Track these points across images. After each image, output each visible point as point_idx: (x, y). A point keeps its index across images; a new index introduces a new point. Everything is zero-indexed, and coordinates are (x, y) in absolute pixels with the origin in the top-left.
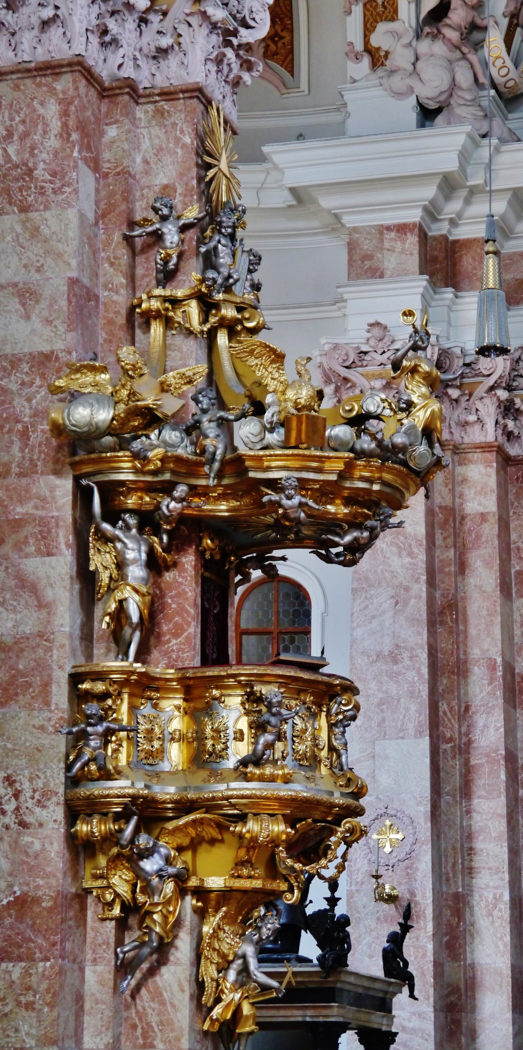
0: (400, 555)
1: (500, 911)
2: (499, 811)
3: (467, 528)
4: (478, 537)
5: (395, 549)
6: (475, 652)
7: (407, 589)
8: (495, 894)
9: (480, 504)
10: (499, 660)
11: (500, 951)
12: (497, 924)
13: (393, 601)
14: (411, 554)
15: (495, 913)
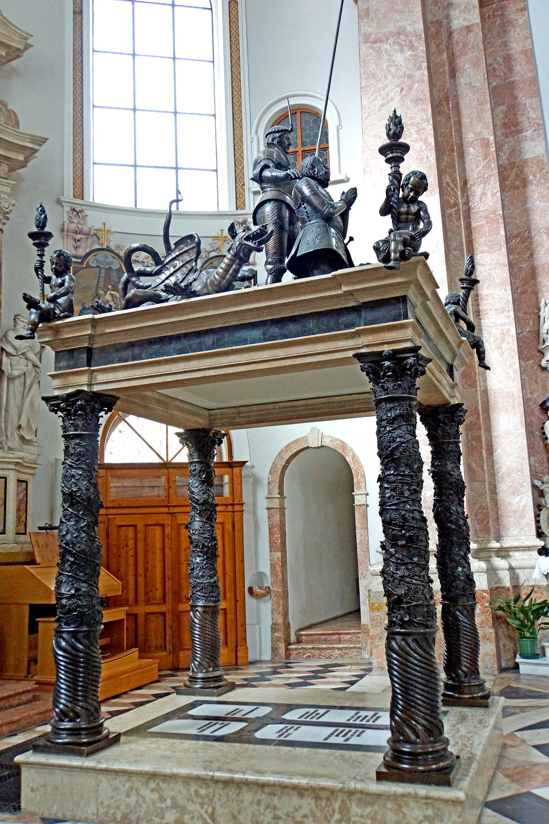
0: (402, 51)
1: (508, 343)
2: (501, 261)
3: (454, 41)
4: (465, 45)
5: (397, 47)
6: (469, 137)
7: (410, 77)
8: (502, 330)
9: (465, 19)
10: (492, 138)
11: (510, 377)
12: (506, 355)
13: (399, 89)
14: (412, 47)
15: (503, 346)
